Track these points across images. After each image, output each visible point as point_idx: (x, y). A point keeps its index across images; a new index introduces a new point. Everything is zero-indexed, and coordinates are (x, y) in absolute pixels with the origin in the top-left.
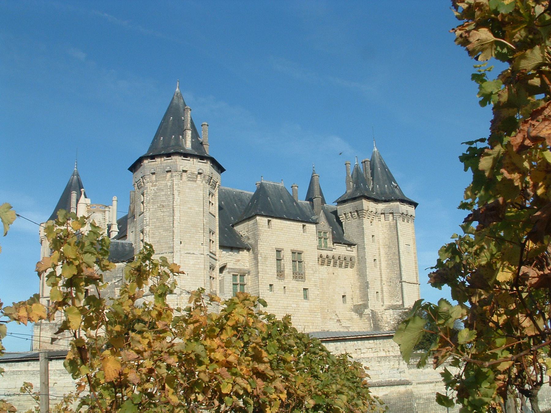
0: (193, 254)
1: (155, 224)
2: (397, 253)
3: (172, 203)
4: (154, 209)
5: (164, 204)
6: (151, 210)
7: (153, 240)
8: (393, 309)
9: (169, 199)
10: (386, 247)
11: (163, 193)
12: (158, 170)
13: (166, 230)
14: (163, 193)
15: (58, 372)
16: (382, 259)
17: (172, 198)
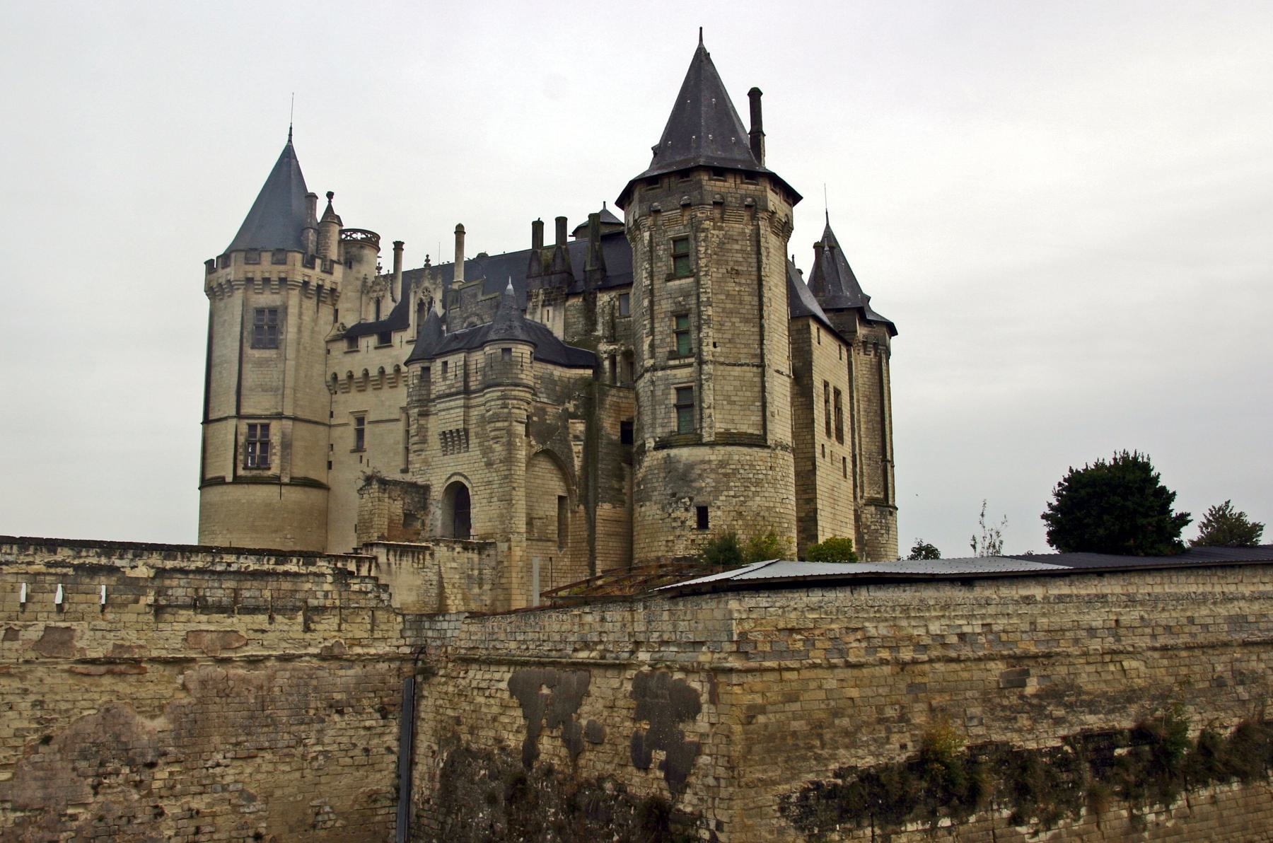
0: (782, 374)
1: (721, 305)
2: (879, 412)
3: (754, 269)
4: (720, 275)
5: (740, 268)
6: (714, 275)
7: (720, 336)
8: (876, 506)
9: (750, 260)
11: (737, 247)
12: (730, 199)
13: (746, 321)
14: (737, 247)
15: (1124, 598)
16: (862, 420)
17: (755, 260)
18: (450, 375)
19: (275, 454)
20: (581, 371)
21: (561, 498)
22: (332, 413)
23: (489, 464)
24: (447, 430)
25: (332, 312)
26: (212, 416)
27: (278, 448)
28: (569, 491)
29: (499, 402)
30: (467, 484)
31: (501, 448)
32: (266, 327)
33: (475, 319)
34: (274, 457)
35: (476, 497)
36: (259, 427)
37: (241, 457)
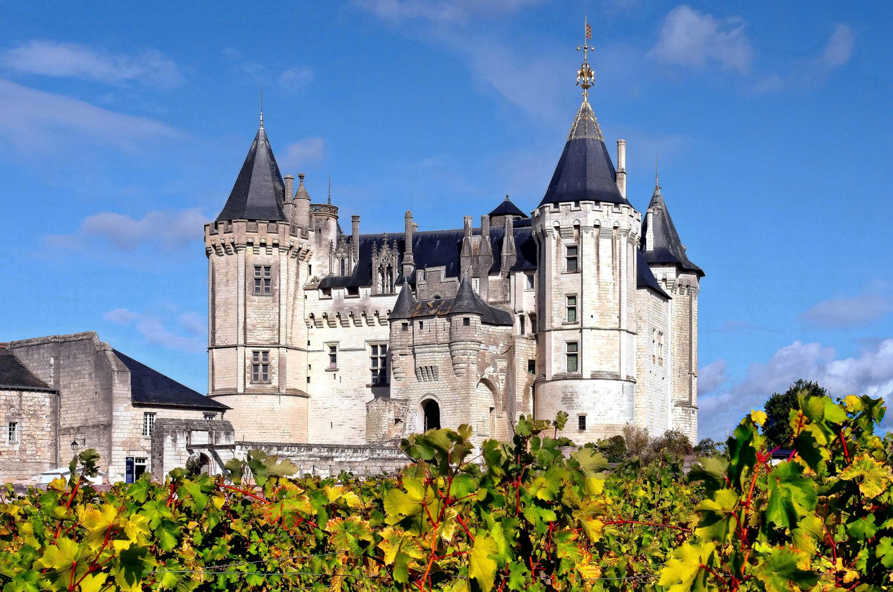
10: (678, 327)
18: (425, 330)
19: (274, 373)
20: (505, 328)
21: (491, 409)
22: (309, 342)
23: (454, 390)
24: (423, 366)
25: (307, 266)
26: (218, 343)
27: (277, 368)
28: (496, 404)
29: (462, 351)
30: (437, 401)
31: (462, 380)
32: (262, 279)
33: (439, 294)
34: (273, 375)
35: (444, 409)
36: (261, 353)
37: (248, 375)
